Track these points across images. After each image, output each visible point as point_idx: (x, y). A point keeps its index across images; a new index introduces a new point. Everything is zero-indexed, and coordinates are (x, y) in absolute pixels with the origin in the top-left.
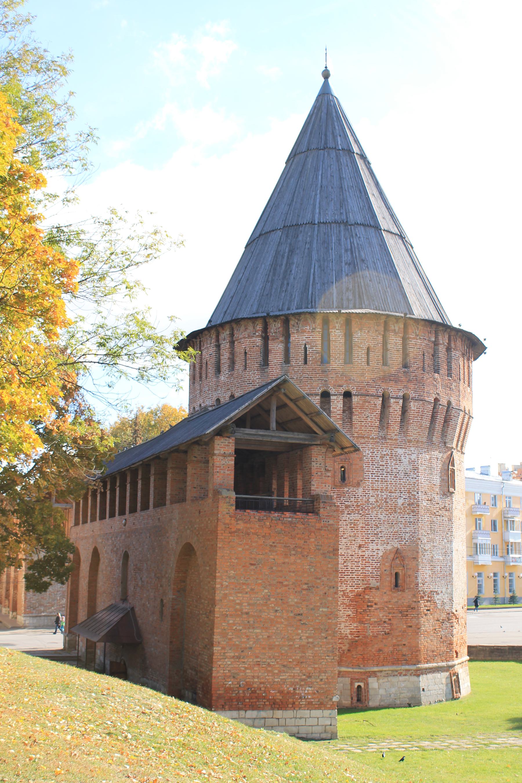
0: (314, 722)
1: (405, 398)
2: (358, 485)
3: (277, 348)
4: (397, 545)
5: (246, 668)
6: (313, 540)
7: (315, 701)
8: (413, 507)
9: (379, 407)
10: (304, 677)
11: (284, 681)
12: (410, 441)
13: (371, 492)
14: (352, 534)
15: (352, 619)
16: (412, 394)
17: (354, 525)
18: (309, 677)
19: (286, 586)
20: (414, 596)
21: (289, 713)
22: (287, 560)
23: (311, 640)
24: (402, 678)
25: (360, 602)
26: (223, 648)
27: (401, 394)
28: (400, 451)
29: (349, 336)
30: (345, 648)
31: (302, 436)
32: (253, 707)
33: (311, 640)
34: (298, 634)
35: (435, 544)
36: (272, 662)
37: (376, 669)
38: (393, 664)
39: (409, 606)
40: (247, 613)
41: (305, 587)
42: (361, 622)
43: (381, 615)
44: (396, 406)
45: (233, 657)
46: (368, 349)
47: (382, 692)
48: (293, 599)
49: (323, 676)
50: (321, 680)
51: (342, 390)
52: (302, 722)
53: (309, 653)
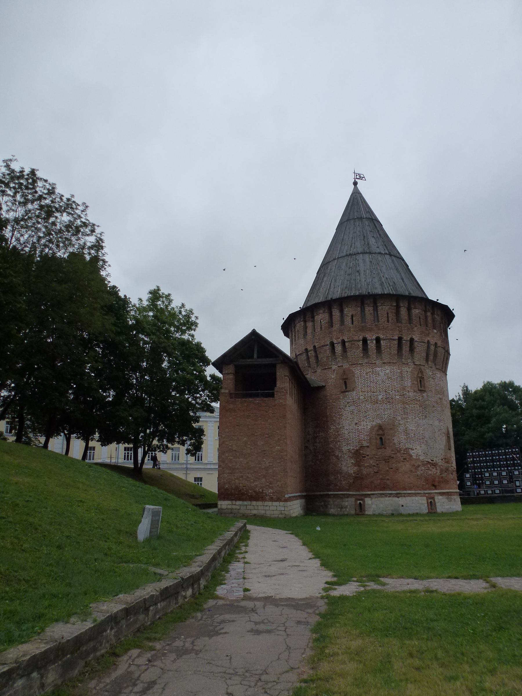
0: (275, 508)
1: (378, 340)
2: (353, 390)
4: (379, 422)
5: (236, 479)
6: (271, 411)
7: (275, 497)
9: (361, 346)
10: (268, 484)
11: (256, 486)
12: (384, 363)
13: (360, 393)
14: (352, 417)
15: (355, 465)
16: (382, 336)
17: (352, 412)
18: (270, 484)
19: (256, 436)
20: (393, 451)
21: (260, 503)
22: (257, 423)
23: (271, 464)
24: (387, 499)
25: (358, 455)
26: (223, 469)
27: (374, 337)
28: (378, 369)
30: (351, 481)
31: (271, 359)
32: (240, 500)
33: (271, 464)
34: (264, 461)
35: (409, 421)
36: (250, 476)
37: (369, 493)
38: (381, 490)
39: (390, 456)
40: (235, 451)
41: (267, 436)
42: (359, 466)
43: (371, 462)
44: (372, 345)
45: (228, 473)
46: (352, 316)
47: (374, 506)
48: (260, 443)
49: (279, 483)
50: (278, 486)
51: (340, 340)
52: (267, 508)
53: (270, 471)
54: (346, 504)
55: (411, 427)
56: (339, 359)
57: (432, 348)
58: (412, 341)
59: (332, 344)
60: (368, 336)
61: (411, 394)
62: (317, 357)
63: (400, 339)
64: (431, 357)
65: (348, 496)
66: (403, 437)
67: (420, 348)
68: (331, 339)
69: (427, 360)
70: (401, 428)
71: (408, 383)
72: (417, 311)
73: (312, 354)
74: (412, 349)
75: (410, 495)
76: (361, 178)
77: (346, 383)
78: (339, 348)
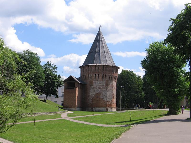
1: (98, 75)
3: (84, 69)
4: (97, 93)
8: (100, 88)
16: (99, 74)
21: (71, 108)
25: (92, 99)
27: (97, 74)
29: (91, 68)
32: (67, 108)
42: (92, 102)
44: (97, 76)
46: (93, 69)
54: (89, 109)
55: (104, 94)
56: (90, 78)
57: (111, 76)
58: (106, 75)
59: (89, 75)
60: (96, 74)
61: (105, 87)
62: (85, 77)
63: (103, 75)
64: (111, 78)
65: (90, 108)
66: (102, 96)
67: (108, 77)
68: (89, 74)
69: (109, 79)
70: (102, 94)
71: (104, 84)
72: (108, 68)
73: (84, 76)
74: (106, 77)
75: (102, 108)
76: (101, 27)
77: (91, 84)
78: (90, 76)
